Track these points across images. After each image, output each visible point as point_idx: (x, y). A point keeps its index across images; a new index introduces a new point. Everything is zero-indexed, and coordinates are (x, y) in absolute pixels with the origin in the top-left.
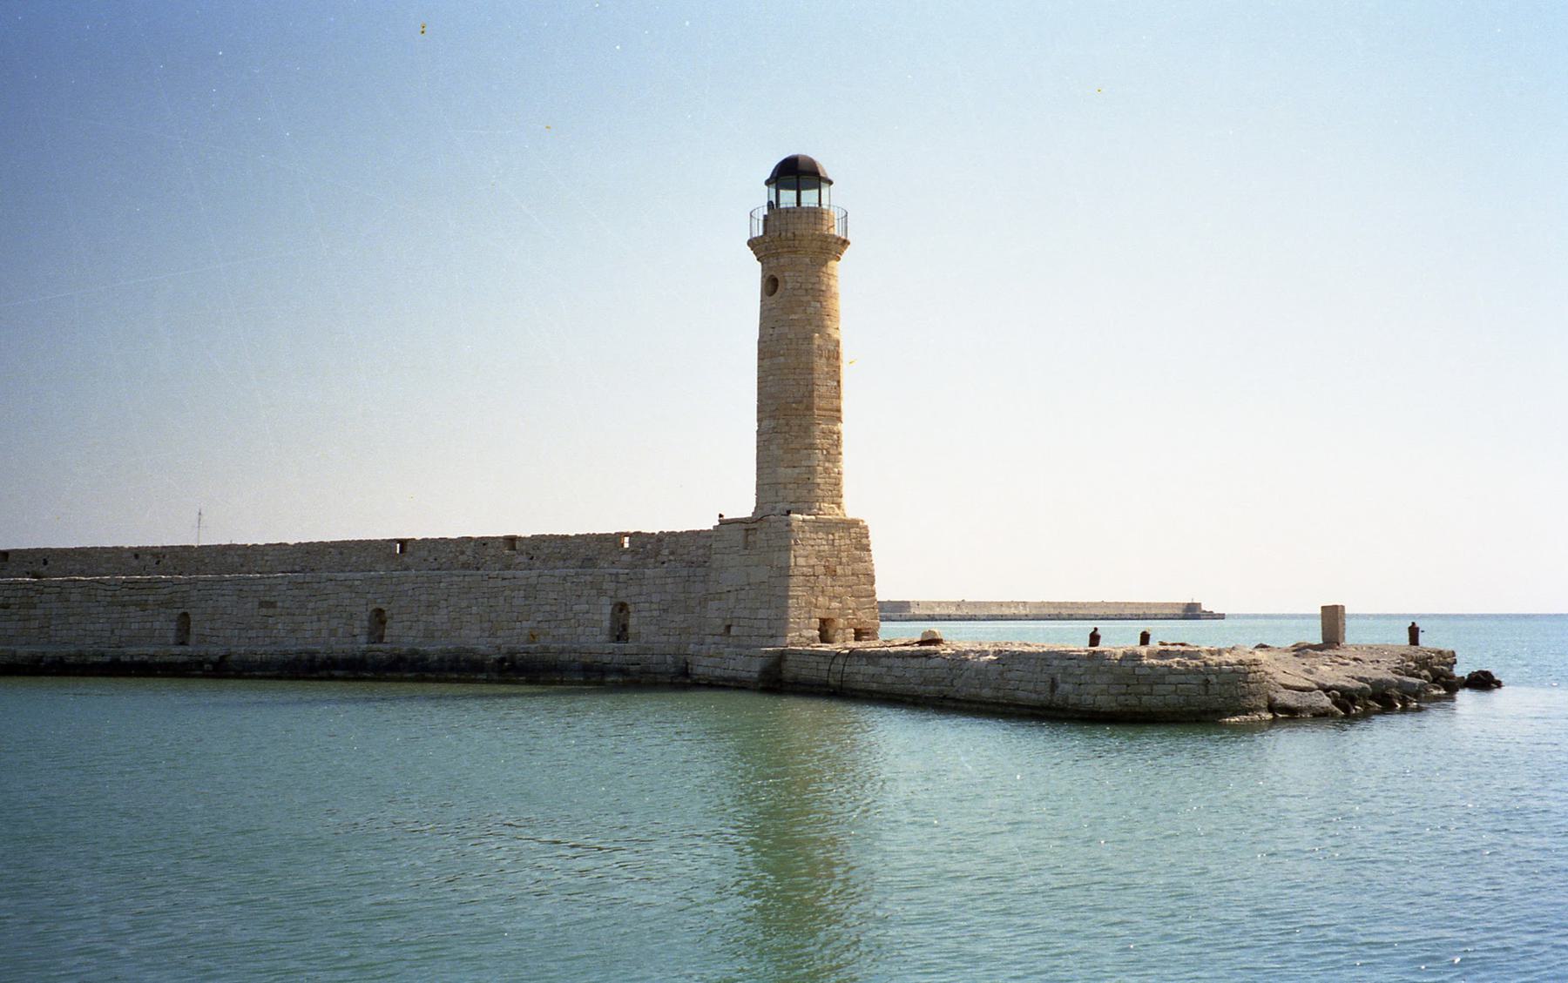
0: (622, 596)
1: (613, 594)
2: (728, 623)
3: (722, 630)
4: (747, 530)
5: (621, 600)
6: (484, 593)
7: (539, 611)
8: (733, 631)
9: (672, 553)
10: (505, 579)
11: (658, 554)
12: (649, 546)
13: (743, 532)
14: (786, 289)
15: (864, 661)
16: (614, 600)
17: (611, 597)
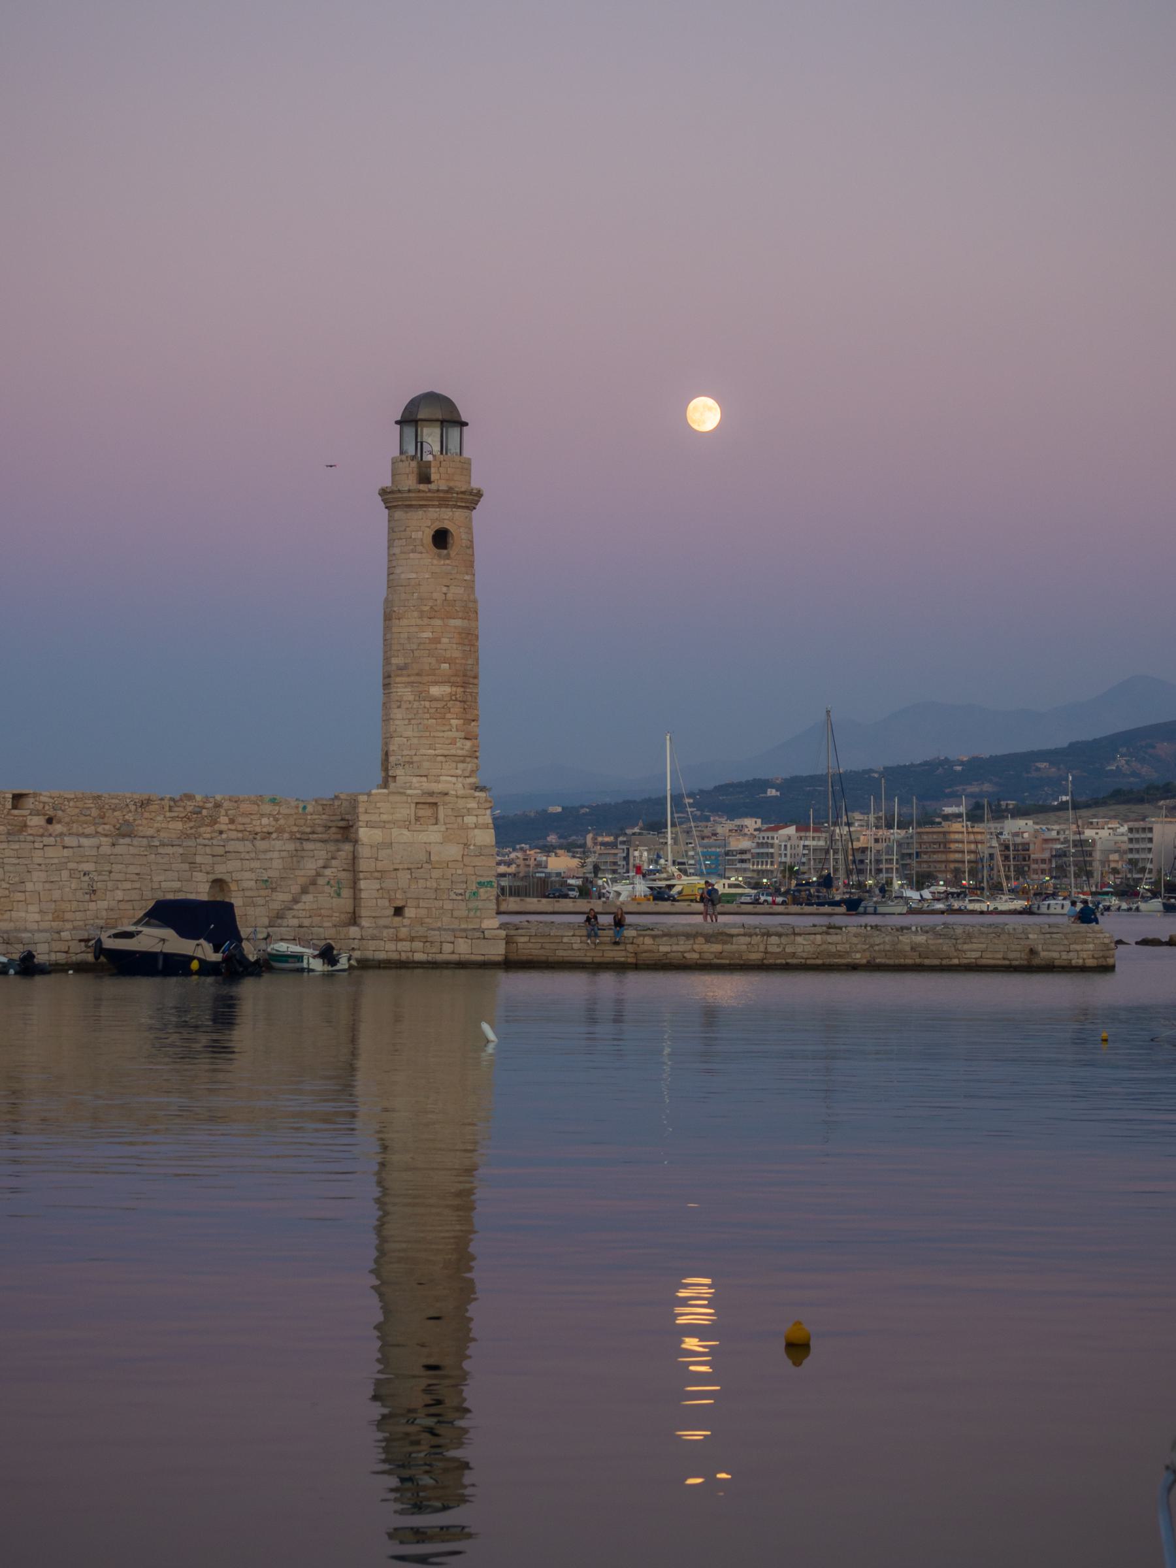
0: (221, 871)
1: (209, 869)
2: (399, 903)
3: (392, 911)
4: (417, 803)
5: (219, 876)
6: (40, 865)
7: (117, 888)
8: (409, 912)
9: (232, 821)
10: (67, 847)
11: (215, 822)
12: (205, 812)
13: (413, 806)
14: (462, 546)
15: (701, 940)
16: (212, 877)
17: (208, 873)
